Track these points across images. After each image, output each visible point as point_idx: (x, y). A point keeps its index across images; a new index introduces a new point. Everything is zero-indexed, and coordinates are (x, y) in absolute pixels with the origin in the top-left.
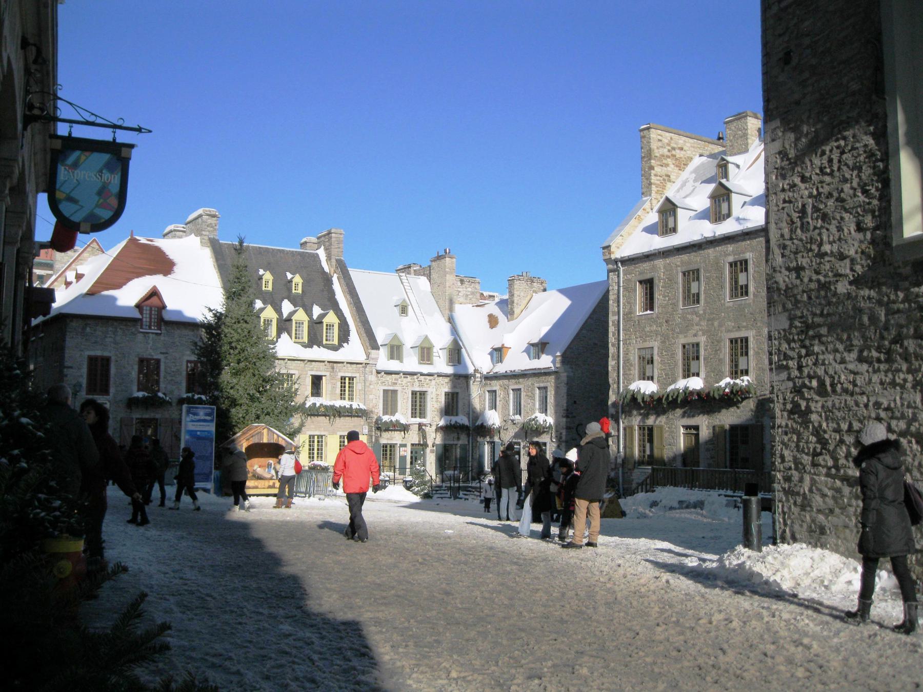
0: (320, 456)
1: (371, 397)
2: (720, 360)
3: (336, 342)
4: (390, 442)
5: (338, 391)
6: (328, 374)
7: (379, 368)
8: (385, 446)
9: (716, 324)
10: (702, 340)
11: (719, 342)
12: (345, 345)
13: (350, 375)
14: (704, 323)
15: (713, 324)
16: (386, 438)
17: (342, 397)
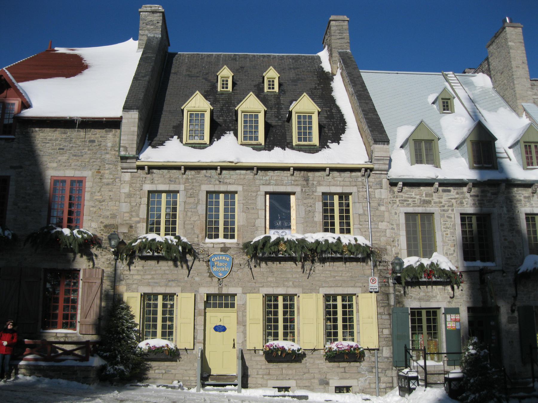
0: (289, 332)
1: (382, 226)
3: (315, 140)
4: (424, 305)
5: (319, 217)
6: (298, 189)
7: (395, 172)
8: (416, 313)
12: (333, 146)
13: (339, 190)
16: (416, 298)
17: (328, 227)
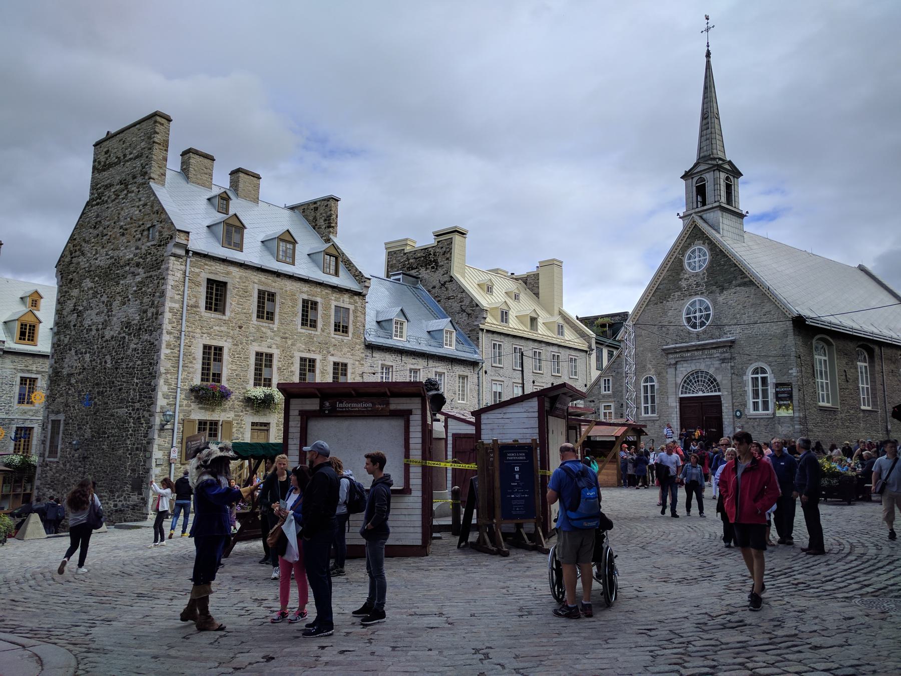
2: (292, 372)
9: (290, 342)
10: (276, 352)
11: (292, 357)
14: (278, 339)
15: (286, 342)
